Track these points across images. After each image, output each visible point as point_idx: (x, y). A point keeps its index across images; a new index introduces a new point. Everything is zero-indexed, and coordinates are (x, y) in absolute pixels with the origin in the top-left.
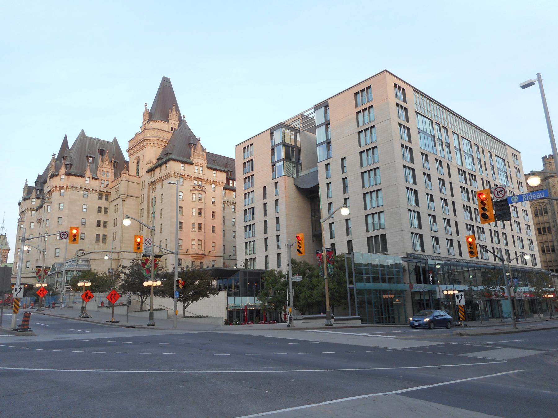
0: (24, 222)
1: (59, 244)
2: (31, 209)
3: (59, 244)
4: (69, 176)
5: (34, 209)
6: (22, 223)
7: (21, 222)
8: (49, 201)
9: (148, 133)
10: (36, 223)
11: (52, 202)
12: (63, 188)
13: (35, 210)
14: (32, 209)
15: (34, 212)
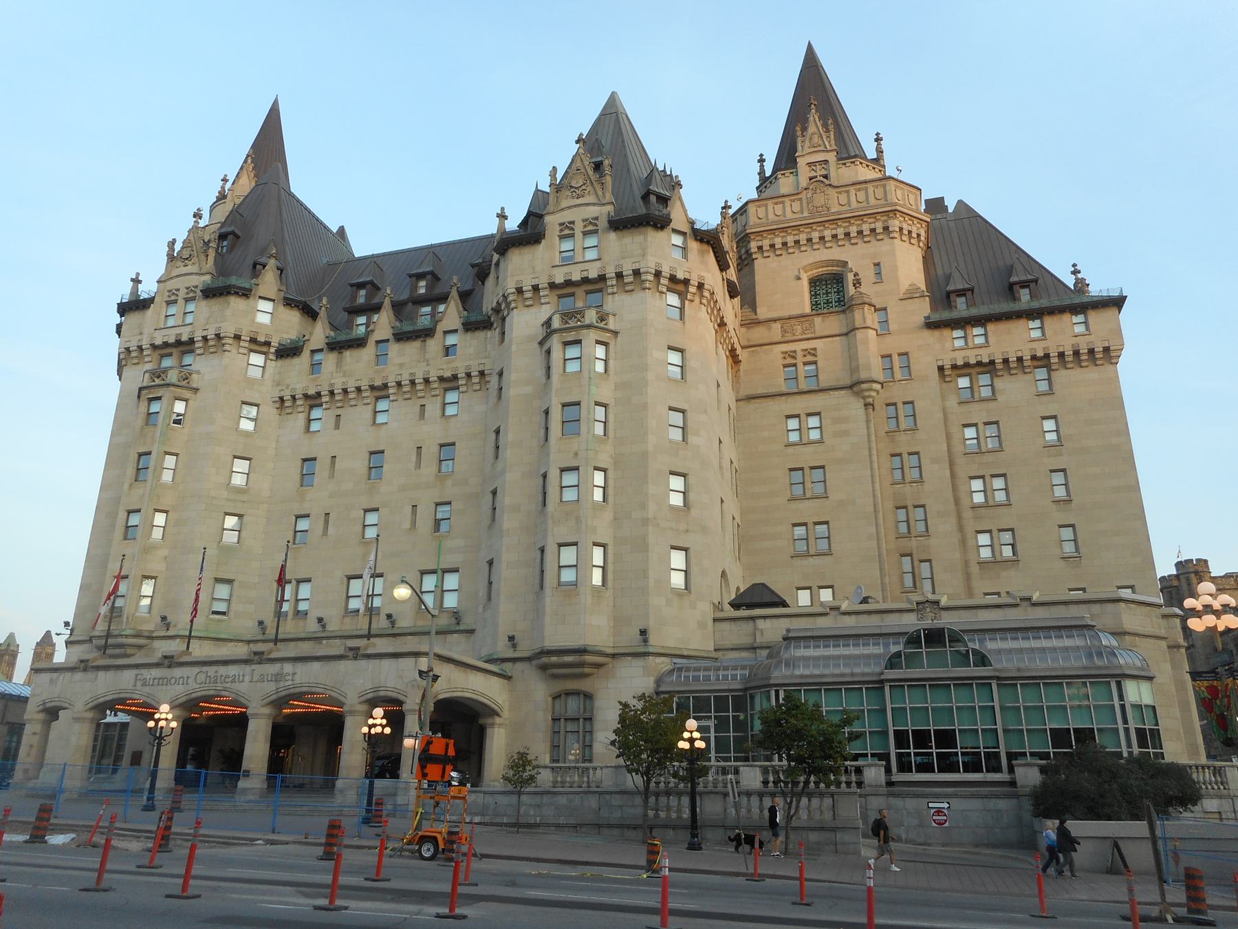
0: (196, 390)
1: (687, 531)
2: (253, 341)
3: (687, 531)
4: (705, 247)
5: (268, 344)
6: (187, 394)
7: (178, 390)
8: (602, 325)
9: (899, 193)
10: (270, 410)
11: (616, 333)
12: (681, 287)
13: (272, 350)
14: (257, 344)
15: (256, 359)
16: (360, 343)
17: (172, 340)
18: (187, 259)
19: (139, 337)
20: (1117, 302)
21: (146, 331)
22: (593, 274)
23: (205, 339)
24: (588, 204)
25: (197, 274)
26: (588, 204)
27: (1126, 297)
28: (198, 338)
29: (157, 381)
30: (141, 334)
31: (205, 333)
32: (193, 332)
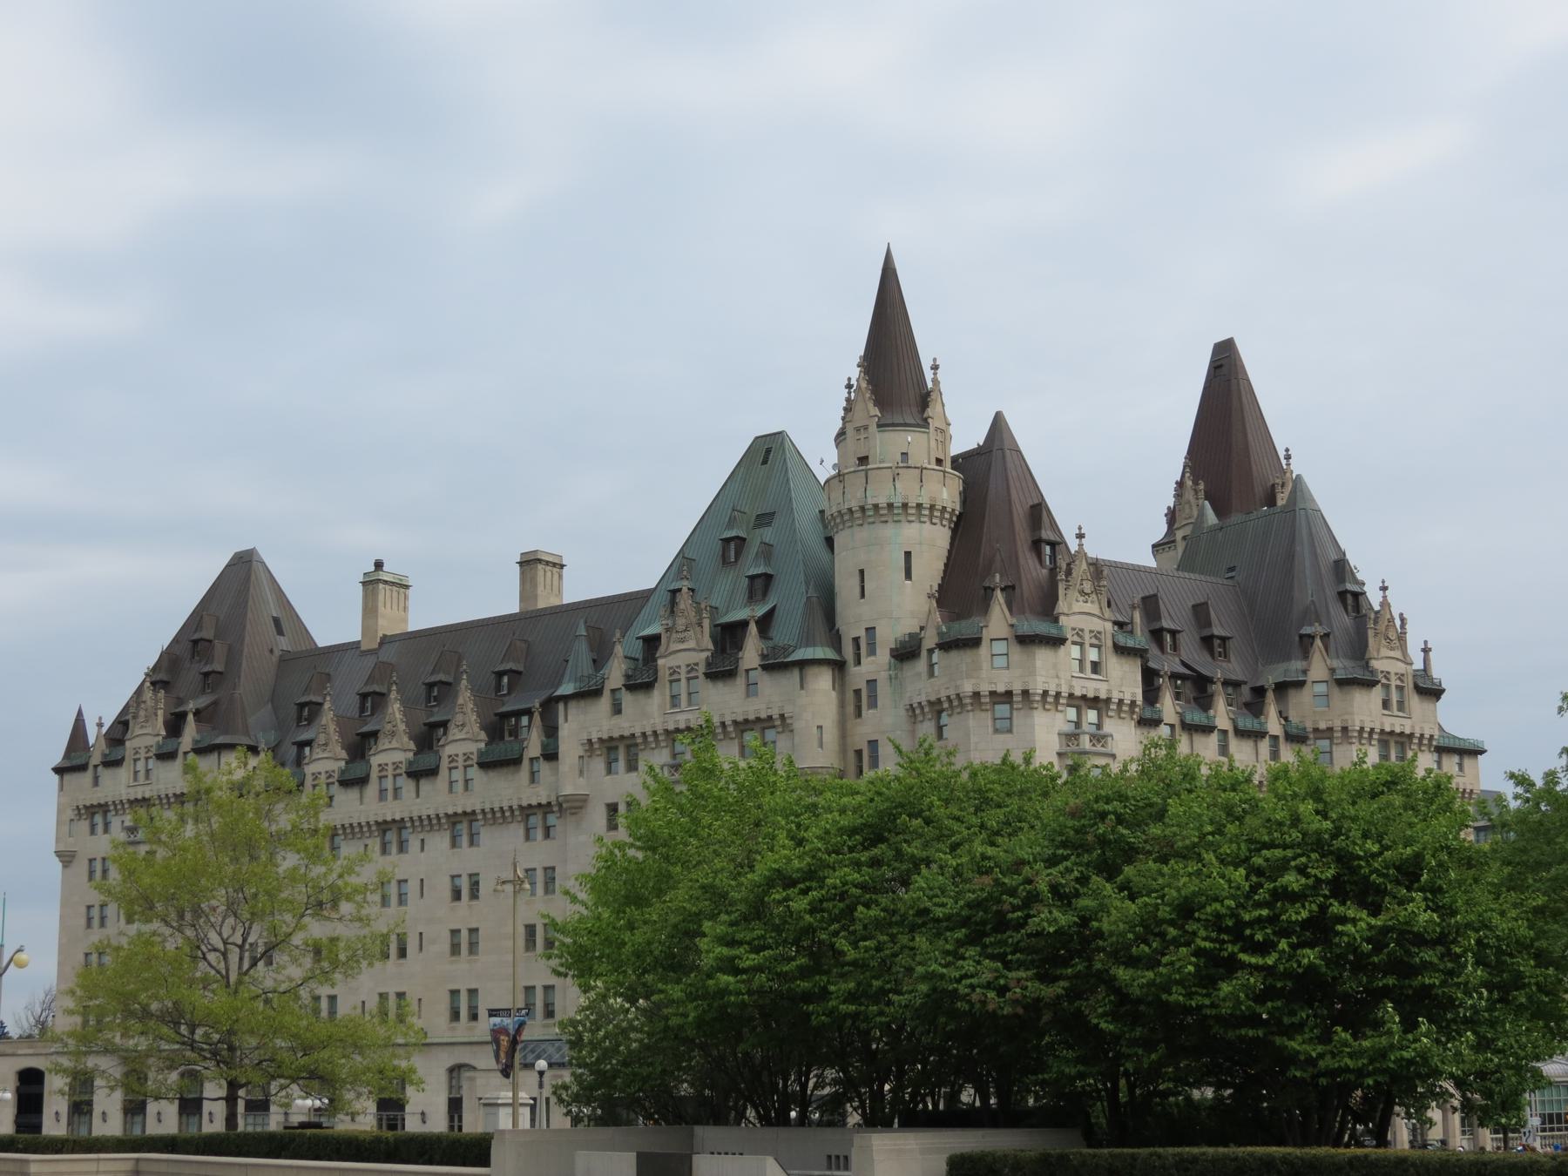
16: (1207, 729)
17: (1091, 695)
18: (1086, 594)
19: (1056, 680)
20: (1475, 752)
21: (1061, 674)
22: (1407, 731)
23: (1121, 702)
24: (1397, 659)
25: (1099, 617)
26: (1397, 659)
27: (1485, 751)
28: (1116, 696)
29: (1099, 748)
30: (1057, 677)
31: (1121, 695)
32: (1109, 691)
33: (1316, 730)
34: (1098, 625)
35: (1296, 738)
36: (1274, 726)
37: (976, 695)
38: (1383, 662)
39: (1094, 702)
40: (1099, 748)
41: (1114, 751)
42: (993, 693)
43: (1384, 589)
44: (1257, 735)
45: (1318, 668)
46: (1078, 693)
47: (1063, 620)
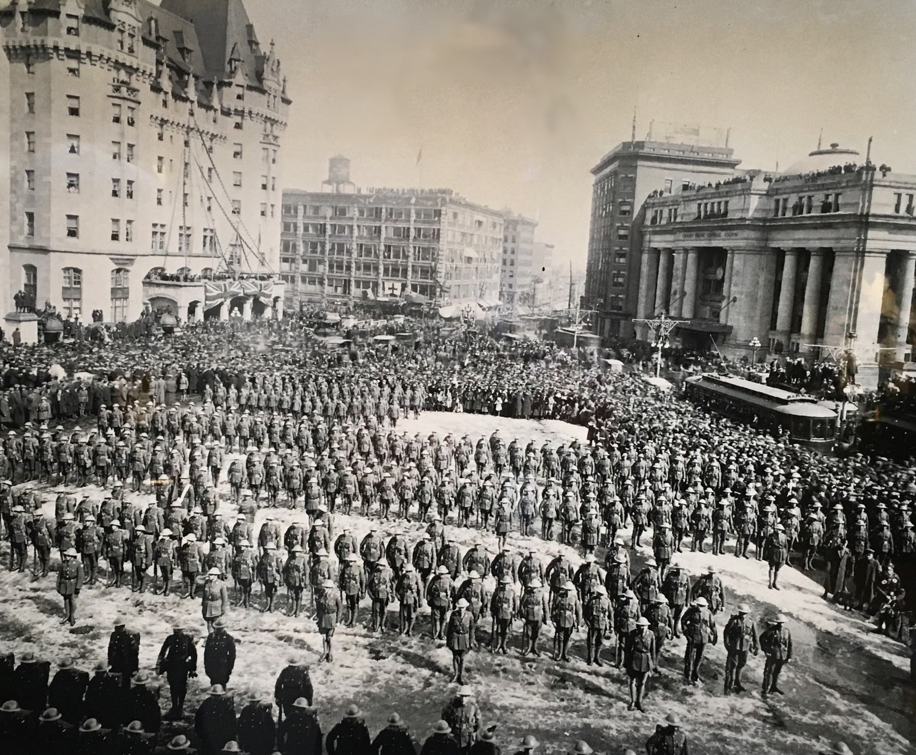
16: (186, 100)
33: (236, 110)
34: (134, 23)
35: (226, 113)
36: (216, 103)
37: (56, 48)
38: (269, 83)
39: (131, 70)
40: (132, 97)
41: (140, 100)
42: (67, 50)
43: (272, 44)
44: (209, 108)
45: (240, 78)
46: (121, 61)
47: (113, 14)
